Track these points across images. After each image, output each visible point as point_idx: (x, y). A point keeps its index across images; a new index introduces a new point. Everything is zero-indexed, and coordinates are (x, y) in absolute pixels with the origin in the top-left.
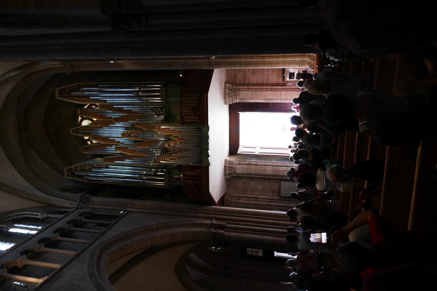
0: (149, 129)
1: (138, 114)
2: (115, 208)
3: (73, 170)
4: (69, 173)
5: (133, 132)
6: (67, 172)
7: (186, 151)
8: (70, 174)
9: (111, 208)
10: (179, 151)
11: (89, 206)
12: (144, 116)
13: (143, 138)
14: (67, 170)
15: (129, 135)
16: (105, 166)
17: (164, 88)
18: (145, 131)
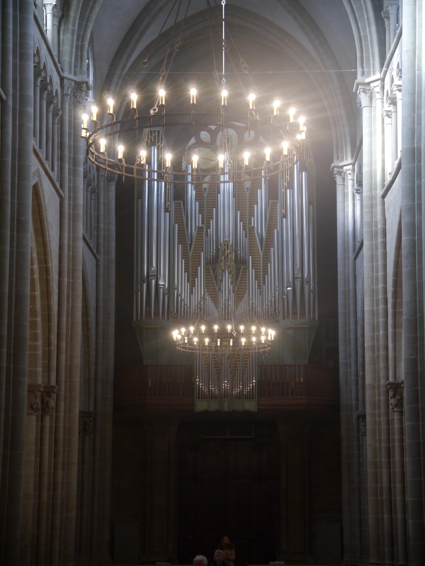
0: (237, 291)
1: (264, 272)
2: (102, 233)
3: (160, 143)
4: (153, 135)
5: (233, 263)
6: (155, 131)
7: (216, 373)
8: (153, 138)
9: (102, 226)
10: (216, 361)
11: (102, 183)
12: (260, 283)
13: (222, 281)
14: (159, 132)
15: (228, 256)
16: (168, 206)
17: (308, 326)
18: (234, 285)
